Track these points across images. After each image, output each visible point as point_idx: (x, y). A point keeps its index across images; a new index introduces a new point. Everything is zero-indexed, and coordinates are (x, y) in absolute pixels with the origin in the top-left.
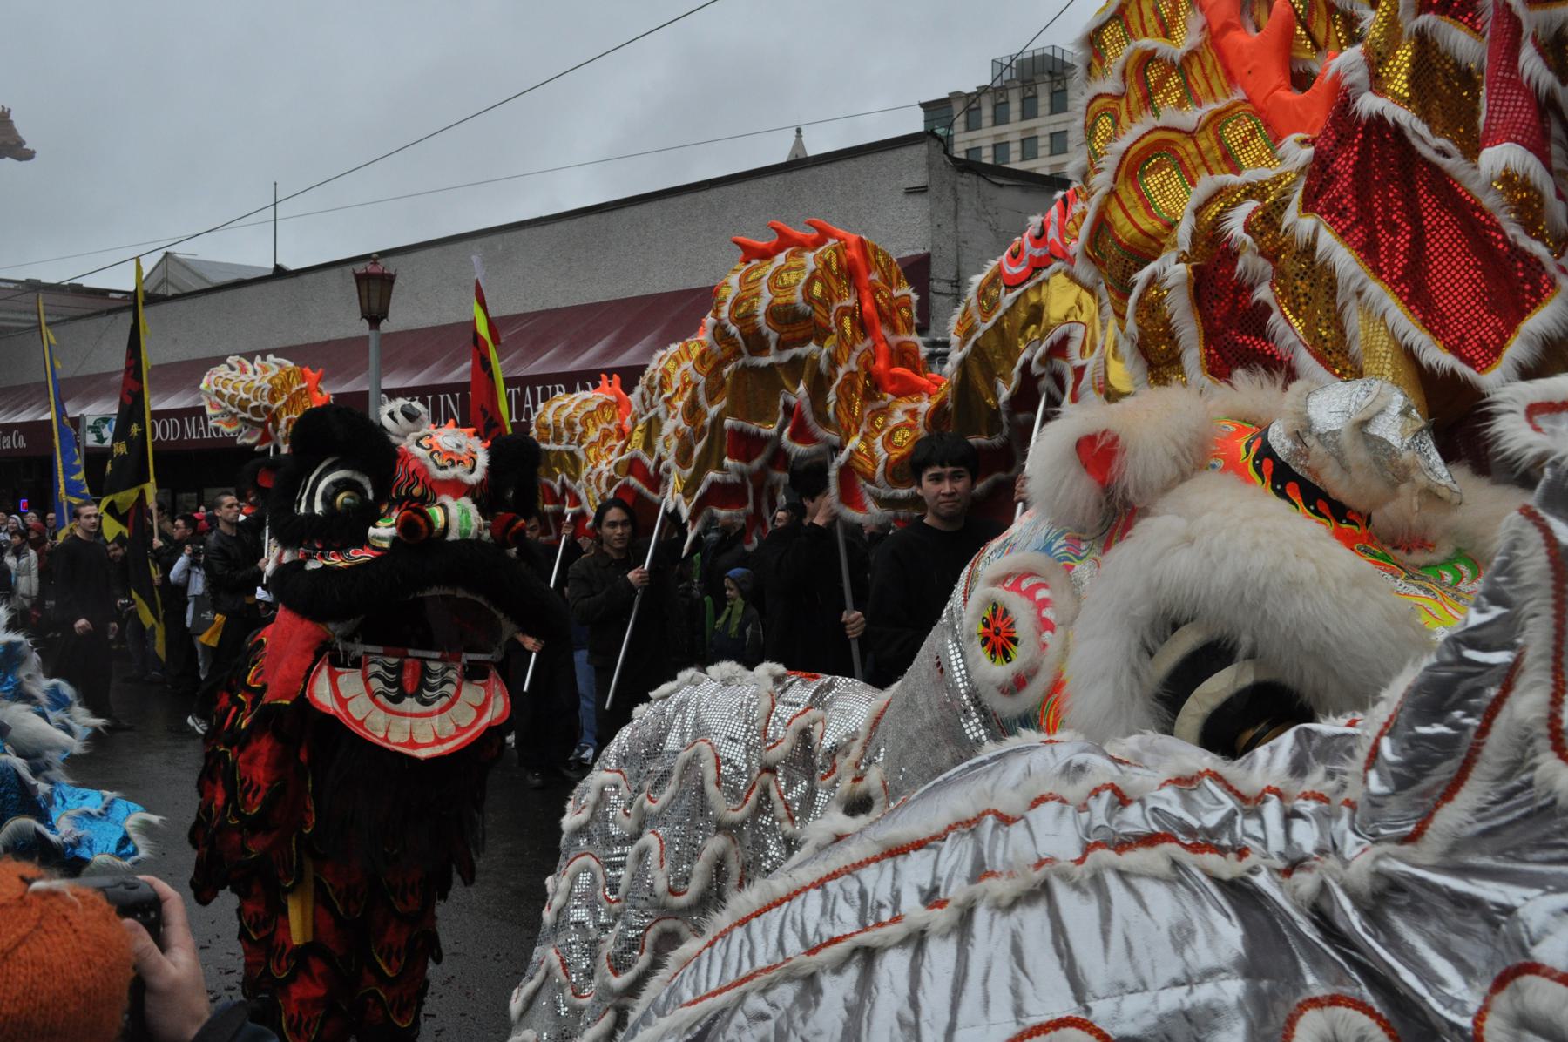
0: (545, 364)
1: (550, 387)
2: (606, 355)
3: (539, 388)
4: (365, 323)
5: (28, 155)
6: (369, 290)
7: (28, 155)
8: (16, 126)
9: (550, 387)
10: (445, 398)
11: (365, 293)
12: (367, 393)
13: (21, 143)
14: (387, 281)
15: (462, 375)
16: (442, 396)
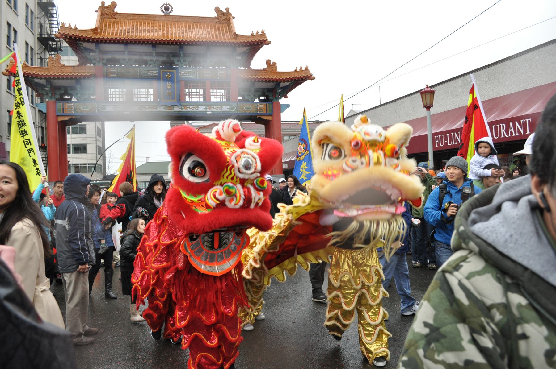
0: (494, 117)
1: (498, 125)
2: (521, 110)
3: (493, 126)
4: (425, 109)
5: (314, 78)
6: (426, 97)
7: (314, 78)
8: (310, 70)
9: (498, 125)
10: (454, 134)
11: (424, 99)
12: (427, 135)
13: (311, 75)
14: (432, 93)
15: (460, 125)
16: (453, 134)
